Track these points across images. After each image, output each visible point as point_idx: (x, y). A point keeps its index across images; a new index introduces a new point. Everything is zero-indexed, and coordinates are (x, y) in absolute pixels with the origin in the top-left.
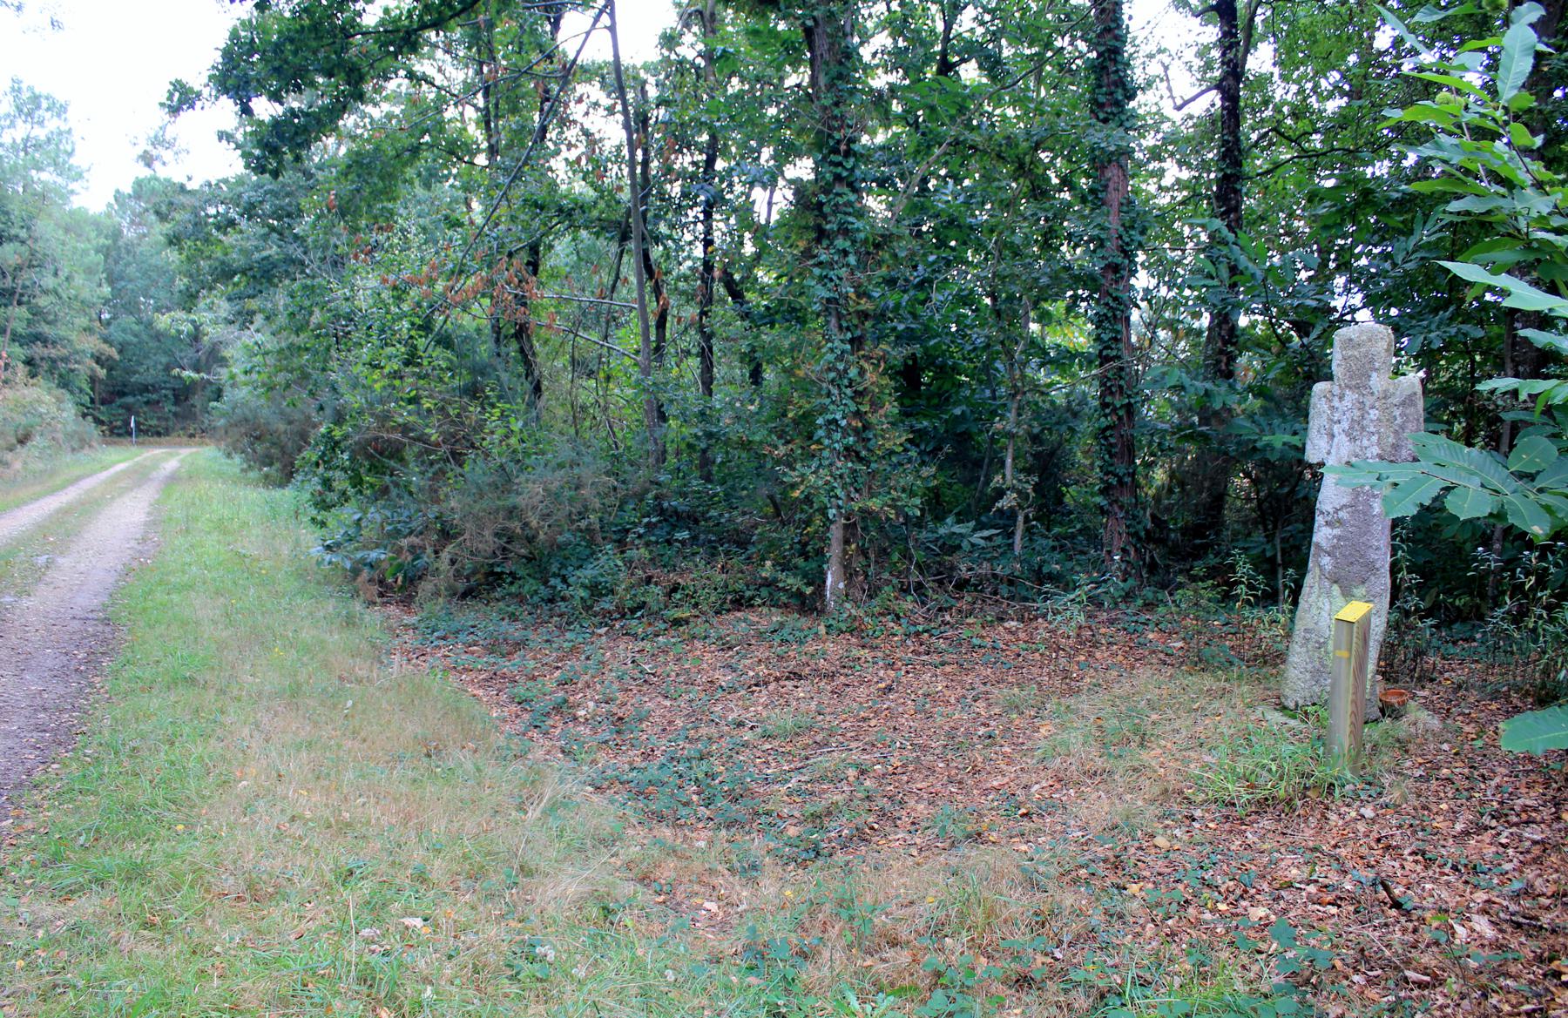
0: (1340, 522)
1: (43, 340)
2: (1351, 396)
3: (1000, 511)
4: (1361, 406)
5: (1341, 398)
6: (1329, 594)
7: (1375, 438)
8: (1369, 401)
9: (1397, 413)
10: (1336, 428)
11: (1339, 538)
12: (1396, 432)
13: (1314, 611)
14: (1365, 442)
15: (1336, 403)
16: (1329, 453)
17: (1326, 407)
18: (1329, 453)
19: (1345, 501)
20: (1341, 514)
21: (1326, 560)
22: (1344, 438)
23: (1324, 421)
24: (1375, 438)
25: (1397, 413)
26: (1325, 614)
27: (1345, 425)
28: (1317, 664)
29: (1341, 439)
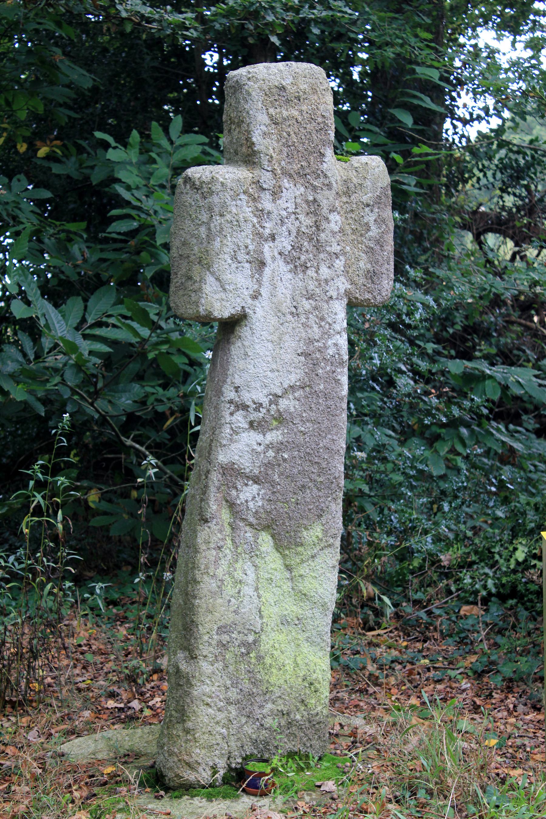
0: (281, 419)
1: (41, 221)
2: (293, 192)
3: (371, 489)
4: (314, 207)
5: (276, 193)
6: (253, 552)
7: (339, 264)
8: (326, 199)
9: (370, 218)
10: (268, 250)
11: (279, 448)
12: (370, 251)
13: (229, 590)
14: (325, 272)
15: (267, 204)
16: (256, 296)
17: (247, 211)
18: (256, 296)
19: (293, 378)
20: (283, 404)
21: (249, 494)
22: (282, 267)
23: (245, 237)
24: (339, 264)
25: (370, 218)
26: (248, 590)
27: (285, 243)
28: (246, 685)
29: (277, 268)
